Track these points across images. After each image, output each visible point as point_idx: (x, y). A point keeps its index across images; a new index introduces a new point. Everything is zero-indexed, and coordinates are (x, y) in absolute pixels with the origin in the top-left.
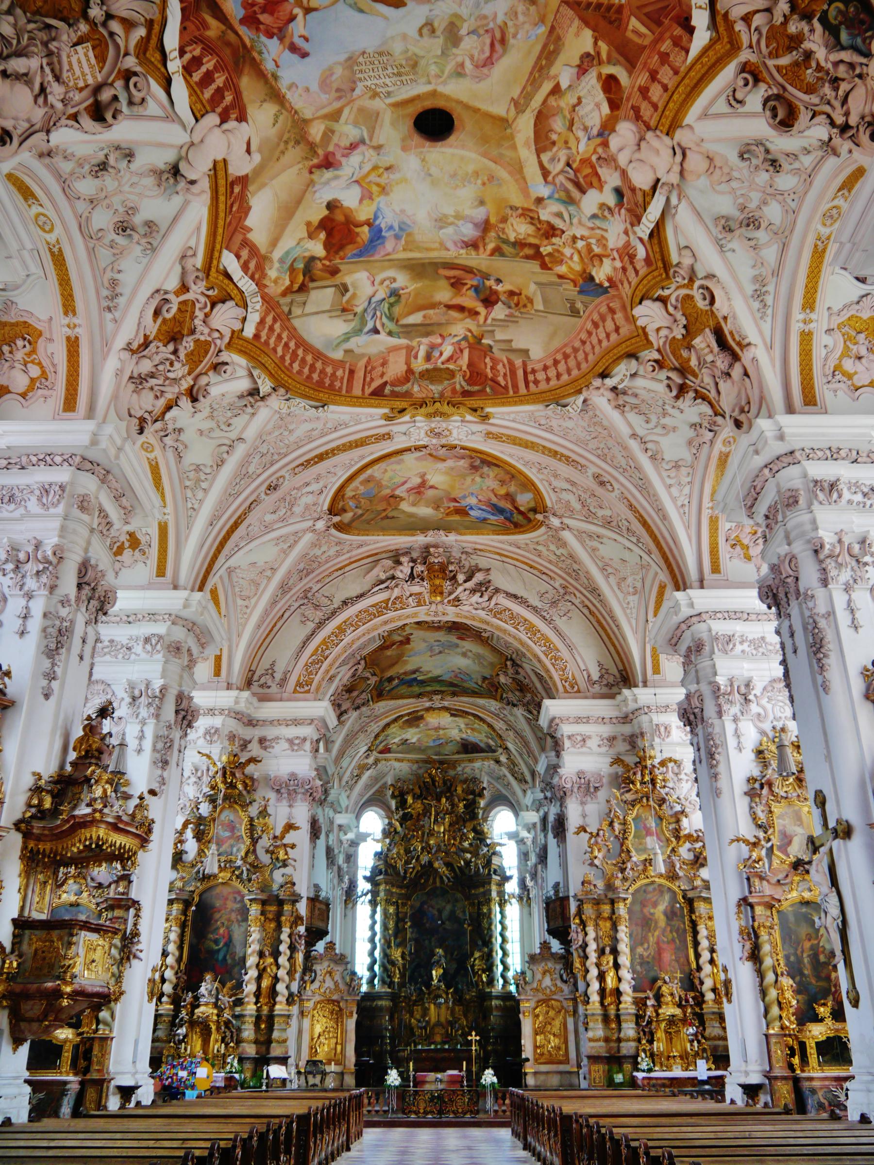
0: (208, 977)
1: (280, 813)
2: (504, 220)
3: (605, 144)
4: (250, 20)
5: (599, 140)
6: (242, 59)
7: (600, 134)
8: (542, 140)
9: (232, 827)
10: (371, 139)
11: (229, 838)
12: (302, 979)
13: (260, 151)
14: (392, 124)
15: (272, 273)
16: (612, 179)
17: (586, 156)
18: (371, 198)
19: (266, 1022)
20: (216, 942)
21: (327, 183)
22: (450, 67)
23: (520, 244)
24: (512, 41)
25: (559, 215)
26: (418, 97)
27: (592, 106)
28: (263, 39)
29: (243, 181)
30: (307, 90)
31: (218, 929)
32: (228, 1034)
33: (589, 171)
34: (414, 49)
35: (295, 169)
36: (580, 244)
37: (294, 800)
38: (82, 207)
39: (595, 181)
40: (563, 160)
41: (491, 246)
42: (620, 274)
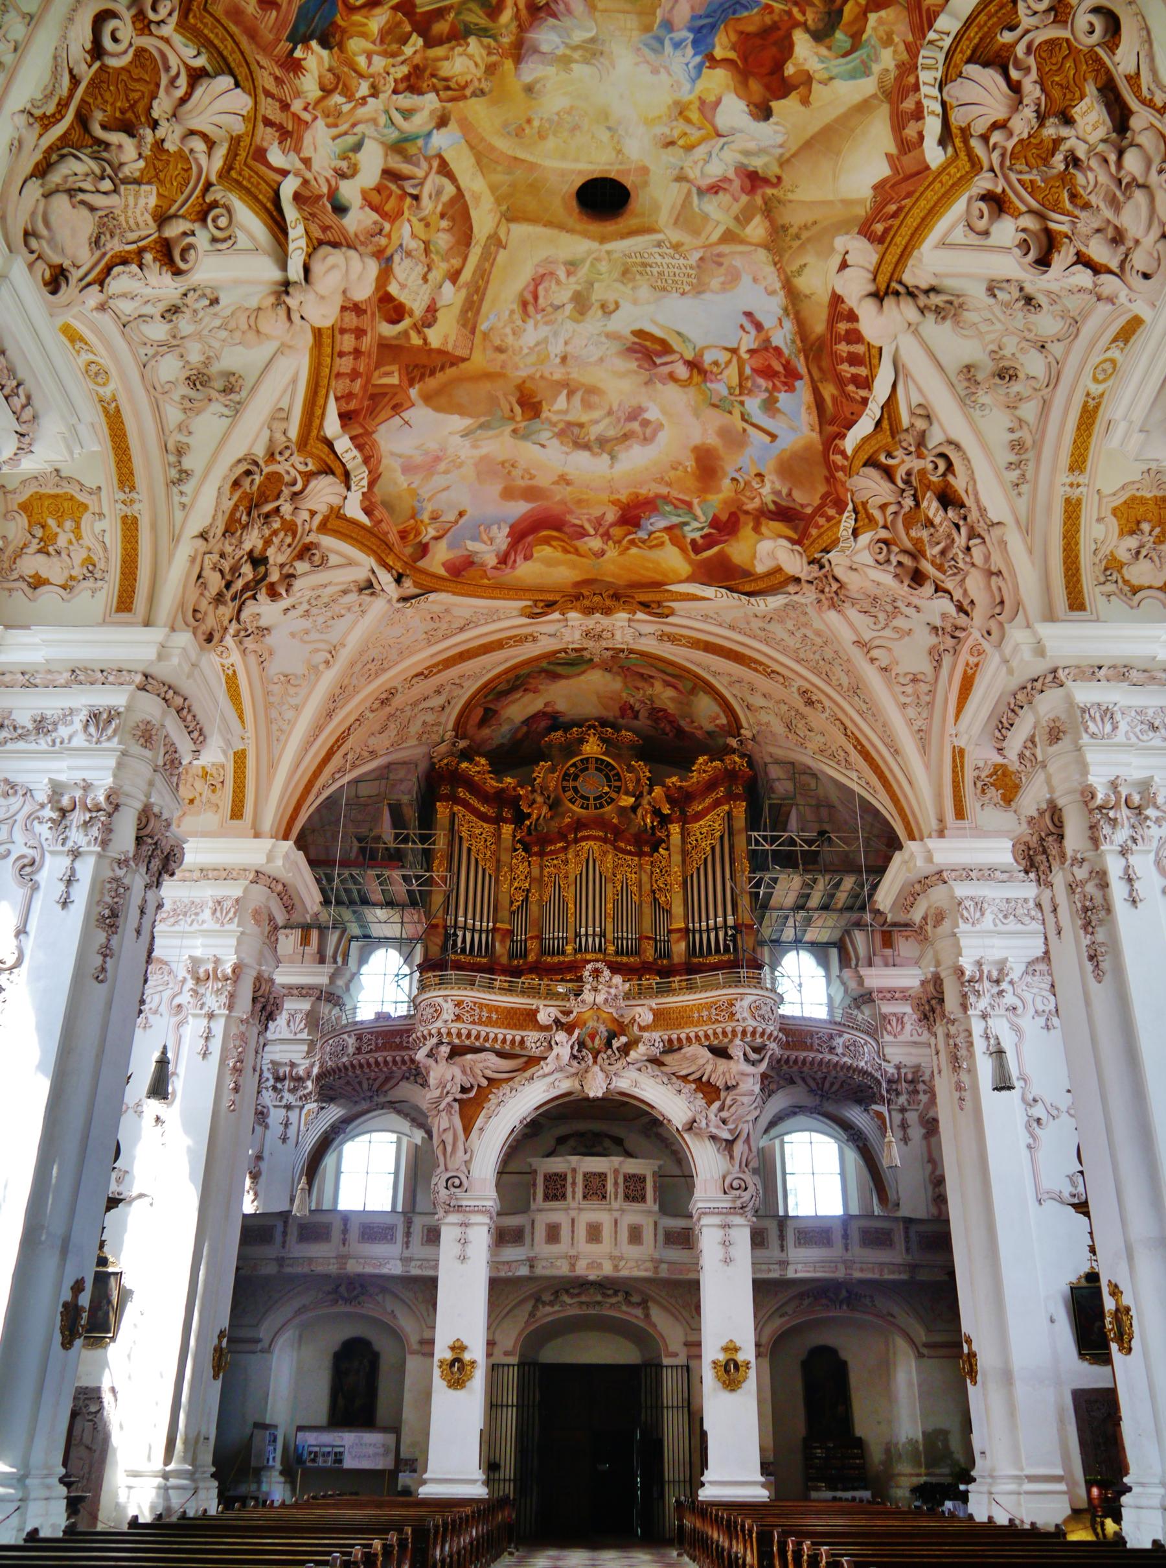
2: (491, 69)
3: (379, 254)
4: (791, 375)
5: (388, 252)
6: (816, 350)
7: (390, 259)
8: (458, 213)
10: (689, 193)
13: (832, 250)
14: (656, 208)
15: (887, 60)
16: (358, 220)
17: (397, 223)
18: (702, 102)
21: (762, 151)
22: (583, 272)
23: (458, 35)
24: (515, 306)
25: (407, 114)
26: (623, 236)
27: (409, 283)
28: (786, 352)
29: (865, 231)
30: (755, 280)
33: (387, 208)
34: (627, 290)
35: (799, 195)
36: (364, 89)
38: (1057, 349)
39: (376, 198)
40: (425, 201)
41: (506, 16)
42: (286, 92)
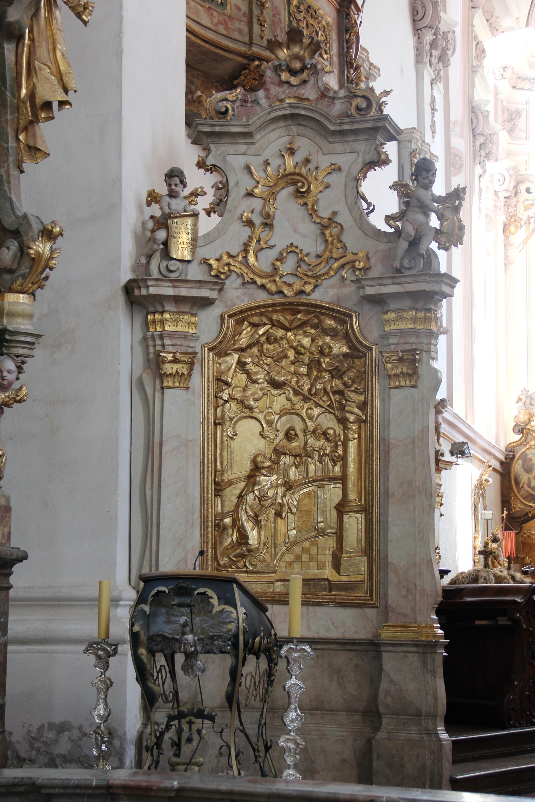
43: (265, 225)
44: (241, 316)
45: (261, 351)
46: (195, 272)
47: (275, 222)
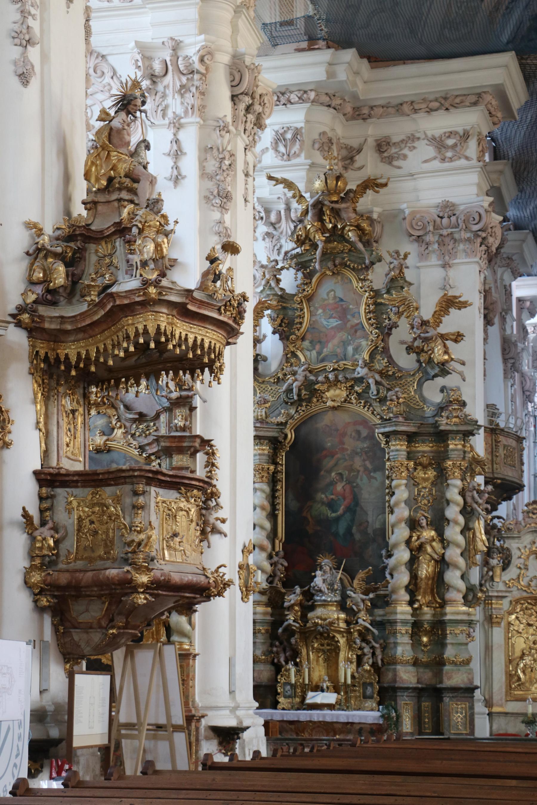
0: (326, 562)
1: (427, 280)
9: (342, 310)
11: (339, 329)
12: (486, 563)
19: (434, 632)
20: (331, 505)
31: (333, 483)
32: (367, 650)
37: (453, 254)
43: (525, 568)
44: (517, 601)
45: (524, 613)
46: (501, 587)
47: (529, 568)
